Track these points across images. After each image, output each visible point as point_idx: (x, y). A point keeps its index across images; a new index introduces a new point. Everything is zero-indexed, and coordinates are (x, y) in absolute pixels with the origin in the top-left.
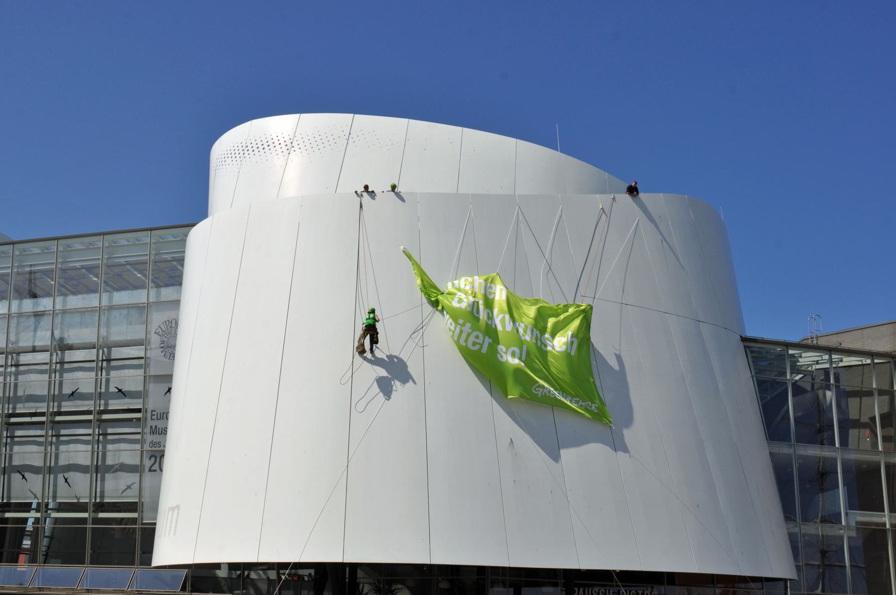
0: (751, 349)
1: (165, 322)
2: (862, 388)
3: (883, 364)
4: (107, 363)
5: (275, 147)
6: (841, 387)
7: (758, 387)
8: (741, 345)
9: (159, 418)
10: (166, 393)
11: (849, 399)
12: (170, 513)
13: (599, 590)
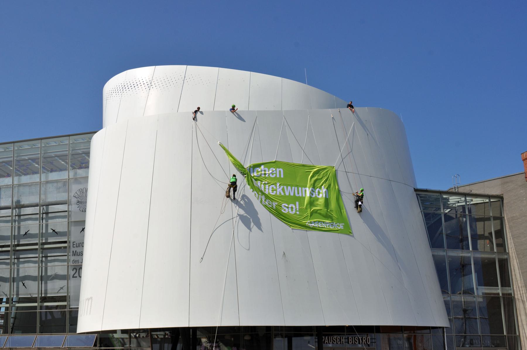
1: (79, 190)
2: (484, 216)
5: (141, 86)
6: (472, 216)
7: (425, 217)
8: (415, 193)
9: (77, 246)
11: (477, 223)
12: (87, 302)
13: (337, 337)
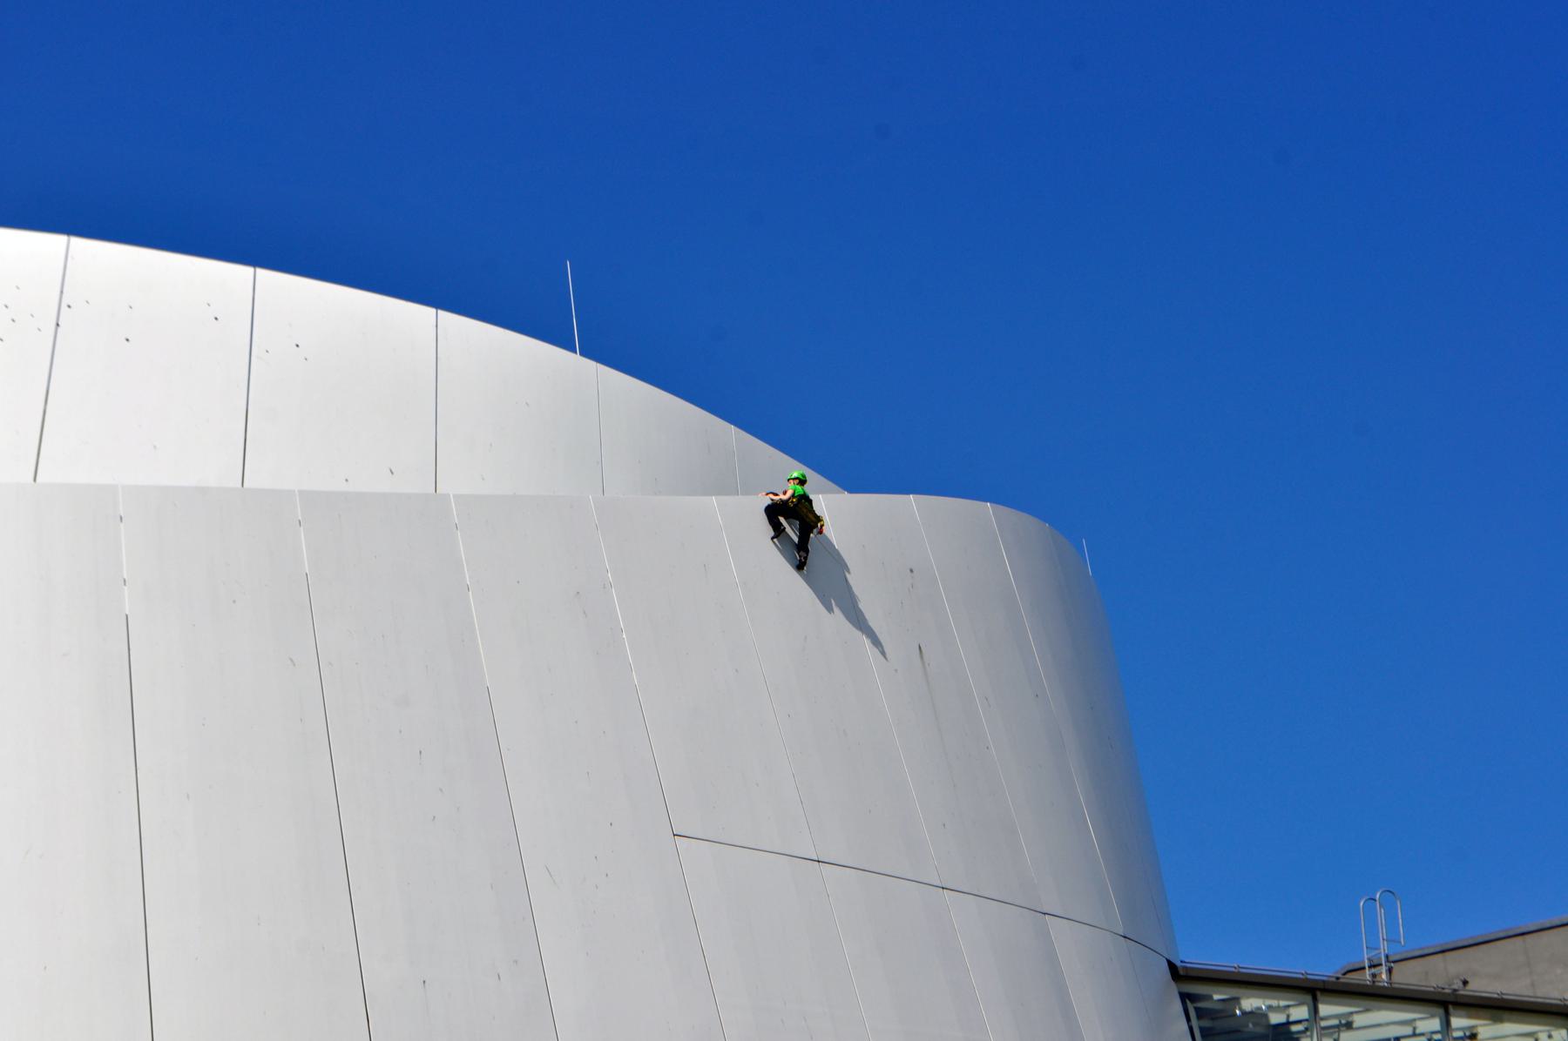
0: (1200, 1005)
8: (1173, 989)
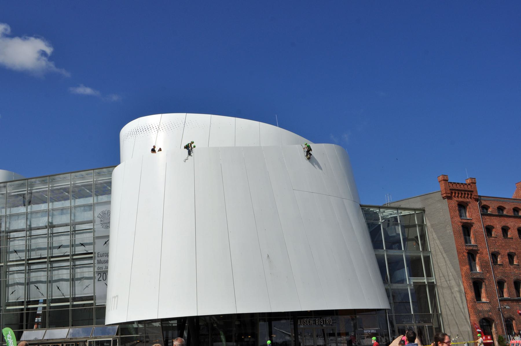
1: (102, 212)
3: (419, 214)
4: (74, 232)
6: (402, 224)
8: (360, 208)
9: (101, 256)
10: (104, 244)
12: (114, 299)
13: (307, 320)
